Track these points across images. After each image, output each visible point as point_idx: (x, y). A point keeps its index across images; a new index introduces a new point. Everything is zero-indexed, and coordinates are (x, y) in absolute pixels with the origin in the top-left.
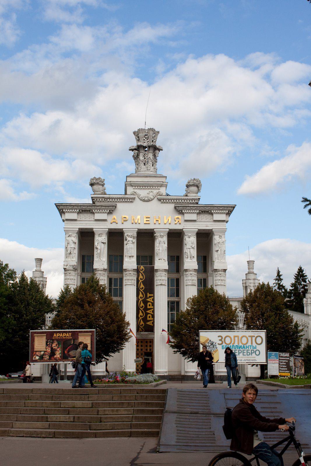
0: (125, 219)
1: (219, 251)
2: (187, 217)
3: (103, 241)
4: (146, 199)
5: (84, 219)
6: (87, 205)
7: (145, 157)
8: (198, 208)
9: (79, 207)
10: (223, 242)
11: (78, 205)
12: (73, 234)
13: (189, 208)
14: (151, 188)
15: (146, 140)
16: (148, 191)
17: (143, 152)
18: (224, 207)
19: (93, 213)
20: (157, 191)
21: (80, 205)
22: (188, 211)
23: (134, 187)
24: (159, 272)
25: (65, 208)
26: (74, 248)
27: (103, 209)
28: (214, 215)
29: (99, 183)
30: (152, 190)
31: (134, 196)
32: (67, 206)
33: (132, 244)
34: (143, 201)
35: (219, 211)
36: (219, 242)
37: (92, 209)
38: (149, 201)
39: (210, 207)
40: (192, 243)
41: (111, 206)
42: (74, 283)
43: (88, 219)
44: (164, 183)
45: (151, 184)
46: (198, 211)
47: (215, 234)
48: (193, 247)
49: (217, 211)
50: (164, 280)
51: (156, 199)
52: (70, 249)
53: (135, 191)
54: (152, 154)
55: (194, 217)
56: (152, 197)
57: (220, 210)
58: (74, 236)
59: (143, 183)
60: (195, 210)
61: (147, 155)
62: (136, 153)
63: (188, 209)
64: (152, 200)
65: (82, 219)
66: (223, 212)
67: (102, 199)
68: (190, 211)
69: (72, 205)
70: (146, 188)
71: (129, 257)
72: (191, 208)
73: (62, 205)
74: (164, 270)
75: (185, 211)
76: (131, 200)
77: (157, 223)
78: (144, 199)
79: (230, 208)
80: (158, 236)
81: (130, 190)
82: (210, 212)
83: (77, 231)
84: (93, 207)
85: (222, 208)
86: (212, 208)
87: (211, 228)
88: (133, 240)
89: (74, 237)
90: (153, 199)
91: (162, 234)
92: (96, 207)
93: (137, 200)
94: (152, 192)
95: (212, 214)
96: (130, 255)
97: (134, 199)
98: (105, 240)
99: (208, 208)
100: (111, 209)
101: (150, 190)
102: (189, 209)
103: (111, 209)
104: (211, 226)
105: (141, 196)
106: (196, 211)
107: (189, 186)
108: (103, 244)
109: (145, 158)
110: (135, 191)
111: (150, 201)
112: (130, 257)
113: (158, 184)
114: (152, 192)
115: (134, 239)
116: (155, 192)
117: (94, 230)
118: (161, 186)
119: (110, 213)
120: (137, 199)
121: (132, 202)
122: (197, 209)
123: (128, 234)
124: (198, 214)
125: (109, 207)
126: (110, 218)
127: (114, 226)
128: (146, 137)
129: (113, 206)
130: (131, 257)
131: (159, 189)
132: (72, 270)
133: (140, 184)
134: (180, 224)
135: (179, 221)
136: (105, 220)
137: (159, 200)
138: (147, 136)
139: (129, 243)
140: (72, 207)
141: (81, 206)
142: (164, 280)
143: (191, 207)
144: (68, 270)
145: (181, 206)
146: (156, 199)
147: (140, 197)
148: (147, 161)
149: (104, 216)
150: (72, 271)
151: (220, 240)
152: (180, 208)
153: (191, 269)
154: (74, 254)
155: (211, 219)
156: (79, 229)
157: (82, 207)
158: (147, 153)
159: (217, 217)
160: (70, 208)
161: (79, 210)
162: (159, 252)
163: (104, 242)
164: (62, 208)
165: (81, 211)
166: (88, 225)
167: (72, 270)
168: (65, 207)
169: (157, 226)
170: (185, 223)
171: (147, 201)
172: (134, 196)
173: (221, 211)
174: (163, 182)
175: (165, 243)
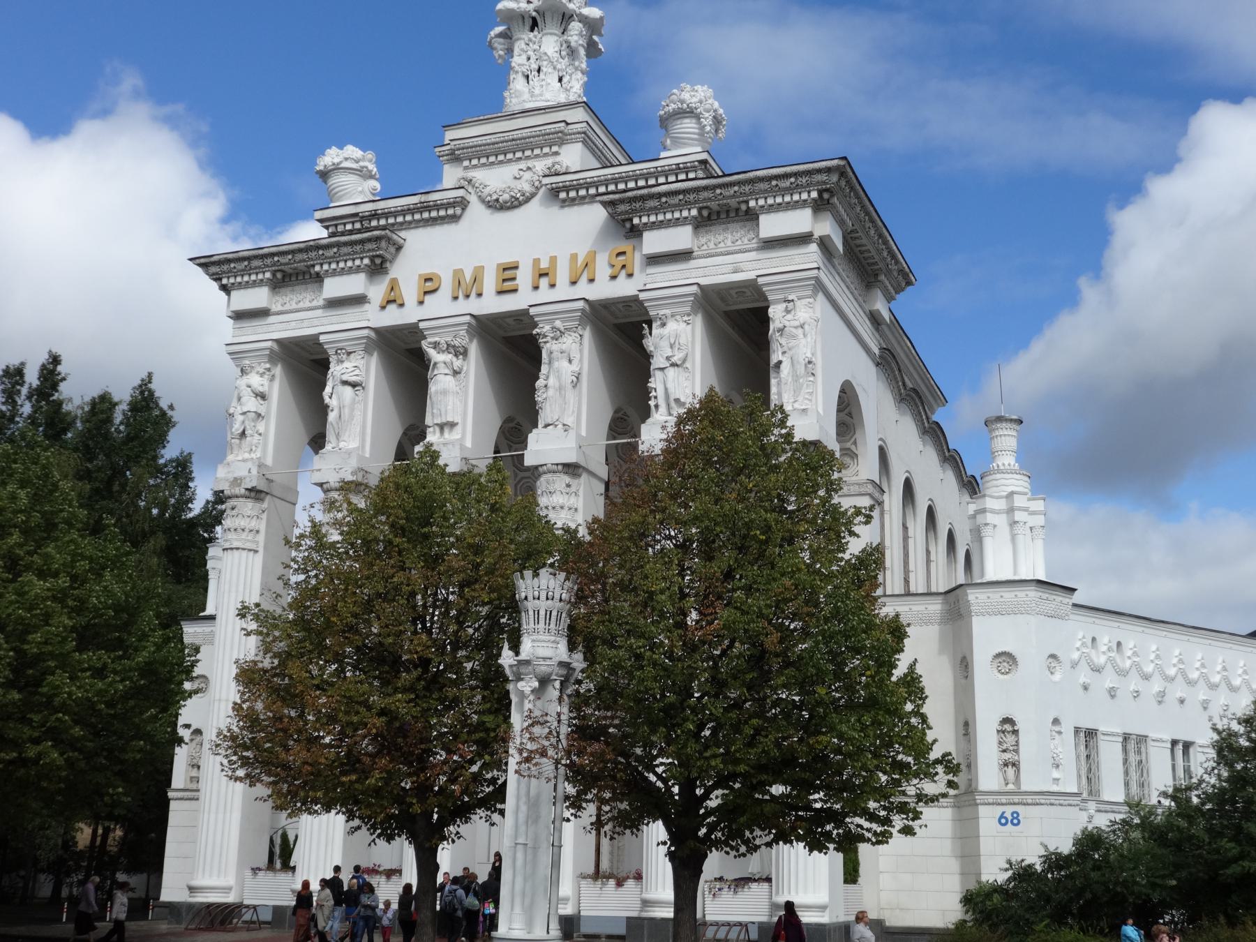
1: (783, 366)
2: (654, 242)
3: (345, 378)
4: (506, 197)
5: (294, 306)
6: (291, 247)
7: (529, 53)
9: (269, 261)
10: (802, 326)
11: (261, 252)
12: (260, 363)
13: (653, 203)
14: (528, 153)
16: (513, 169)
18: (796, 175)
19: (319, 279)
20: (549, 161)
21: (266, 251)
22: (653, 218)
23: (466, 163)
24: (543, 479)
25: (224, 272)
26: (259, 415)
27: (345, 255)
28: (763, 218)
29: (342, 165)
30: (530, 163)
31: (461, 193)
32: (229, 261)
33: (450, 378)
34: (496, 208)
35: (779, 200)
36: (781, 326)
37: (312, 260)
38: (513, 204)
39: (739, 183)
40: (672, 346)
41: (369, 240)
42: (253, 547)
43: (308, 304)
44: (570, 127)
45: (525, 138)
46: (694, 212)
47: (770, 298)
48: (675, 359)
49: (770, 201)
50: (562, 508)
52: (241, 418)
53: (471, 174)
54: (556, 38)
55: (680, 238)
56: (528, 188)
57: (784, 191)
58: (262, 371)
59: (493, 139)
60: (680, 207)
61: (536, 47)
63: (651, 209)
64: (528, 200)
65: (288, 304)
66: (796, 197)
67: (353, 223)
68: (661, 217)
69: (241, 254)
70: (510, 156)
71: (437, 429)
72: (662, 201)
73: (213, 259)
74: (560, 467)
75: (645, 219)
76: (450, 212)
77: (544, 282)
78: (497, 200)
79: (823, 177)
80: (545, 336)
82: (744, 207)
84: (313, 254)
85: (786, 184)
86: (747, 188)
87: (750, 275)
88: (454, 359)
89: (262, 375)
90: (533, 195)
91: (558, 324)
92: (321, 252)
93: (476, 208)
94: (529, 168)
95: (751, 217)
96: (439, 422)
97: (463, 203)
98: (357, 372)
99: (731, 191)
100: (373, 250)
101: (523, 165)
102: (656, 208)
103: (373, 250)
104: (755, 265)
105: (486, 191)
106: (685, 213)
107: (667, 119)
108: (348, 389)
109: (529, 59)
110: (471, 174)
111: (520, 204)
112: (442, 427)
113: (549, 134)
114: (529, 168)
115: (456, 355)
116: (540, 166)
117: (322, 339)
118: (562, 142)
119: (378, 268)
120: (476, 208)
121: (455, 218)
122: (688, 205)
123: (437, 339)
124: (702, 223)
126: (377, 292)
127: (393, 318)
129: (378, 239)
130: (446, 430)
131: (556, 153)
132: (242, 496)
133: (485, 145)
134: (630, 275)
135: (624, 266)
137: (554, 192)
139: (436, 372)
140: (246, 263)
141: (273, 255)
142: (562, 508)
143: (660, 195)
144: (230, 497)
145: (622, 201)
147: (484, 195)
148: (535, 66)
150: (244, 500)
151: (789, 317)
152: (622, 208)
154: (257, 437)
155: (754, 241)
156: (277, 341)
157: (276, 259)
158: (535, 37)
159: (772, 225)
160: (240, 267)
161: (274, 274)
162: (544, 396)
164: (217, 274)
165: (279, 275)
166: (306, 323)
167: (242, 496)
168: (225, 267)
169: (545, 294)
170: (651, 270)
171: (509, 208)
172: (461, 193)
173: (787, 199)
174: (568, 124)
175: (570, 361)
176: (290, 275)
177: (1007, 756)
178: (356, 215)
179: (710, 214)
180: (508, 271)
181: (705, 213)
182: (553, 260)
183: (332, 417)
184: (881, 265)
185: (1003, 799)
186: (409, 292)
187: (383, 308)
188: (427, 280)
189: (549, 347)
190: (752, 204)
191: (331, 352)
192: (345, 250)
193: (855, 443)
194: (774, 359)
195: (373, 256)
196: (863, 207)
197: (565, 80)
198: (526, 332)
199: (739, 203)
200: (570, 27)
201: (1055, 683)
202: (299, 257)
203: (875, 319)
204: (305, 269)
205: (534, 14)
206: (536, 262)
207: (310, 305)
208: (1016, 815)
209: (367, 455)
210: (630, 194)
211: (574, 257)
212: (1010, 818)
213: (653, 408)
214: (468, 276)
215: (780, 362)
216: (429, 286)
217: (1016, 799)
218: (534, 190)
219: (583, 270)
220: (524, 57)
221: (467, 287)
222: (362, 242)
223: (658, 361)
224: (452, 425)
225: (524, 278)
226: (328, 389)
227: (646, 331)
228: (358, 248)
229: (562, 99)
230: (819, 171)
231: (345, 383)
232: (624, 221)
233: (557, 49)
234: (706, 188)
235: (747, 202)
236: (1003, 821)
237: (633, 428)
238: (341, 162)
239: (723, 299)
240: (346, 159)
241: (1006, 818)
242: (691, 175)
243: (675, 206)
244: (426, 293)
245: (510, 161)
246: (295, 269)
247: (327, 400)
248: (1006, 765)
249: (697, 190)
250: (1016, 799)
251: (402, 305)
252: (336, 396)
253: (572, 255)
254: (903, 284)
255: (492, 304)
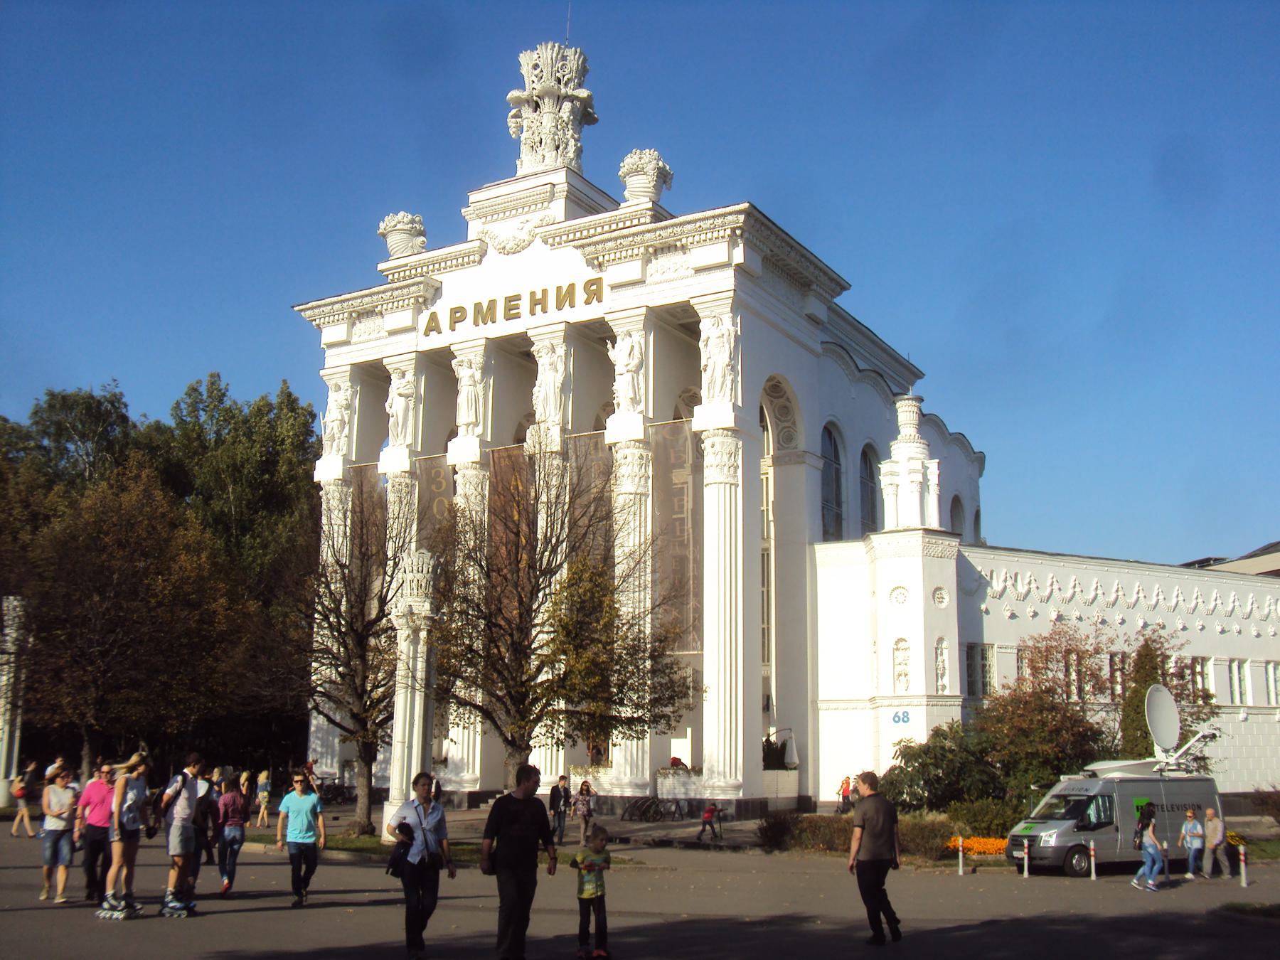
0: (458, 315)
3: (401, 391)
8: (638, 238)
15: (536, 81)
17: (527, 116)
20: (540, 215)
23: (484, 219)
41: (413, 285)
51: (538, 240)
54: (553, 115)
55: (631, 270)
56: (527, 238)
59: (500, 200)
62: (514, 125)
77: (539, 308)
78: (504, 248)
81: (475, 228)
82: (678, 244)
83: (348, 374)
84: (375, 298)
86: (678, 229)
101: (524, 218)
108: (403, 398)
110: (487, 227)
111: (523, 248)
112: (468, 425)
116: (535, 218)
117: (385, 362)
125: (412, 289)
127: (435, 342)
128: (537, 71)
129: (420, 283)
131: (548, 208)
136: (412, 329)
138: (539, 70)
146: (538, 240)
148: (538, 139)
149: (403, 318)
153: (624, 443)
156: (353, 365)
163: (406, 392)
174: (554, 185)
176: (363, 314)
177: (899, 669)
178: (406, 265)
179: (655, 251)
180: (512, 303)
181: (651, 250)
182: (545, 292)
183: (391, 420)
184: (814, 279)
185: (896, 702)
186: (444, 321)
187: (427, 334)
188: (455, 313)
189: (543, 361)
190: (684, 241)
191: (391, 371)
192: (396, 293)
193: (794, 423)
194: (703, 363)
195: (418, 297)
196: (777, 236)
197: (561, 148)
198: (525, 349)
199: (676, 241)
200: (563, 106)
201: (940, 609)
202: (366, 300)
203: (812, 319)
204: (372, 309)
205: (535, 98)
206: (533, 294)
207: (378, 336)
208: (906, 714)
209: (419, 450)
210: (595, 239)
211: (559, 288)
212: (901, 716)
213: (615, 406)
214: (485, 307)
215: (706, 366)
216: (457, 315)
217: (906, 702)
218: (531, 238)
219: (566, 297)
220: (530, 132)
221: (484, 314)
222: (408, 286)
223: (618, 370)
224: (476, 424)
225: (524, 305)
226: (389, 401)
227: (609, 346)
228: (405, 291)
229: (541, 168)
230: (730, 214)
231: (400, 395)
232: (593, 259)
233: (554, 124)
234: (649, 231)
235: (680, 240)
236: (897, 719)
237: (785, 393)
238: (395, 226)
239: (673, 315)
240: (399, 223)
241: (899, 717)
242: (642, 220)
243: (627, 246)
244: (455, 322)
245: (515, 216)
246: (365, 309)
247: (388, 409)
248: (900, 675)
249: (643, 233)
250: (906, 702)
251: (440, 333)
252: (396, 404)
253: (475, 304)
254: (838, 289)
255: (502, 328)
